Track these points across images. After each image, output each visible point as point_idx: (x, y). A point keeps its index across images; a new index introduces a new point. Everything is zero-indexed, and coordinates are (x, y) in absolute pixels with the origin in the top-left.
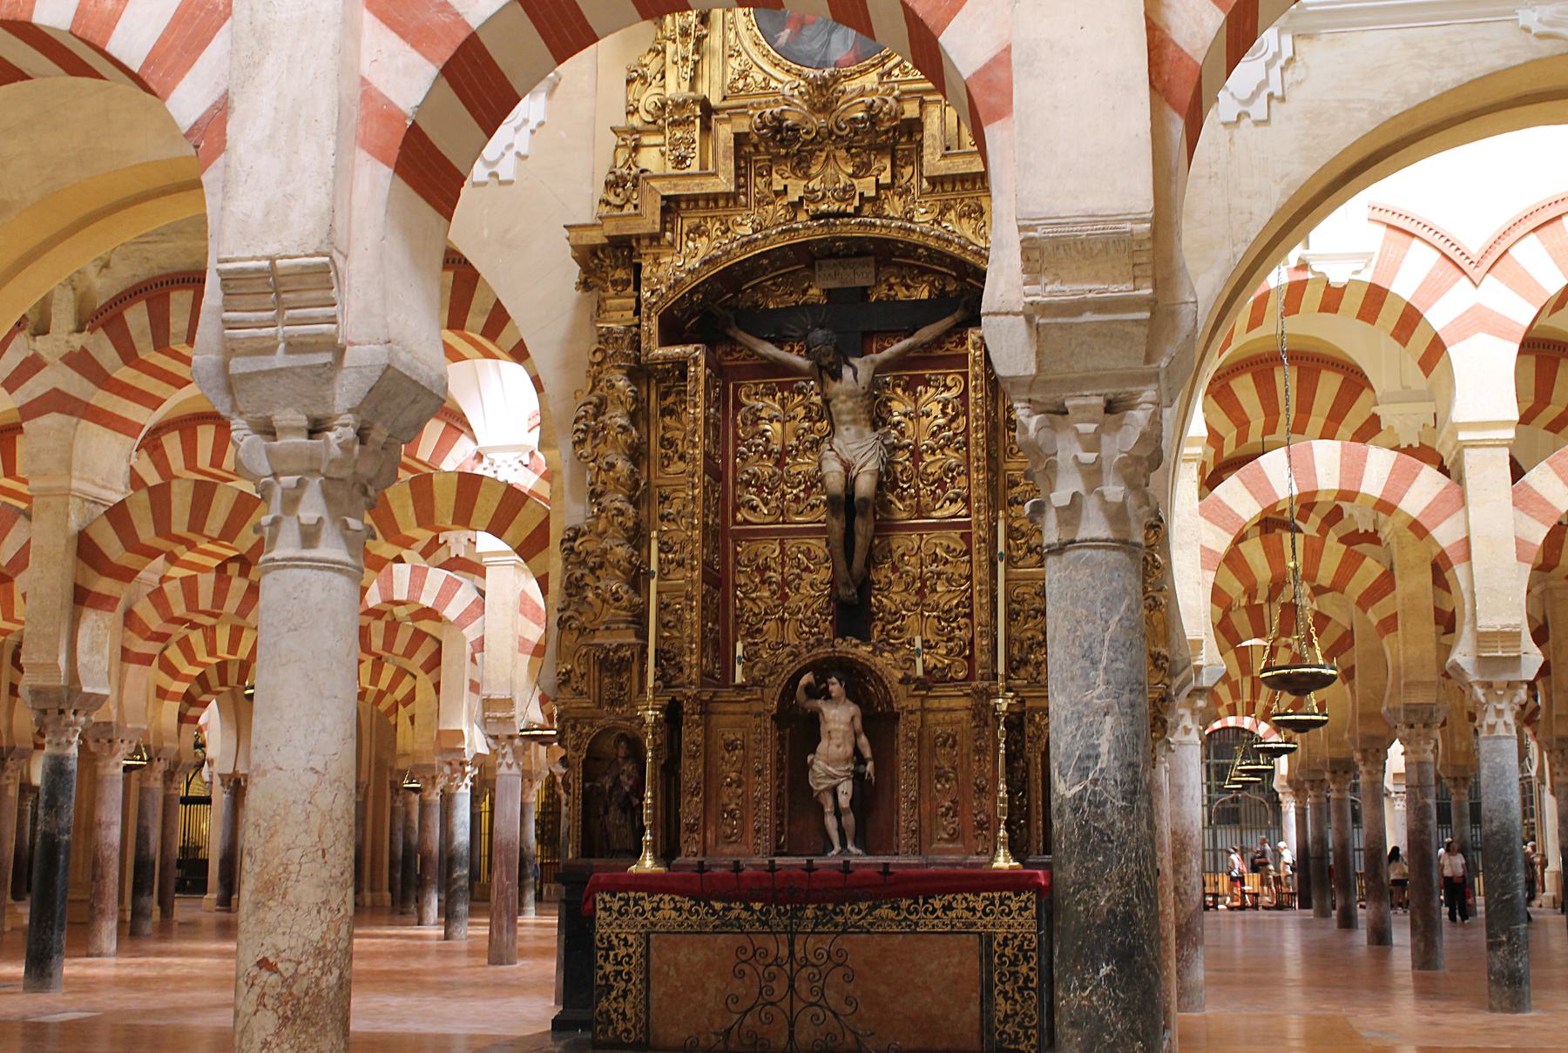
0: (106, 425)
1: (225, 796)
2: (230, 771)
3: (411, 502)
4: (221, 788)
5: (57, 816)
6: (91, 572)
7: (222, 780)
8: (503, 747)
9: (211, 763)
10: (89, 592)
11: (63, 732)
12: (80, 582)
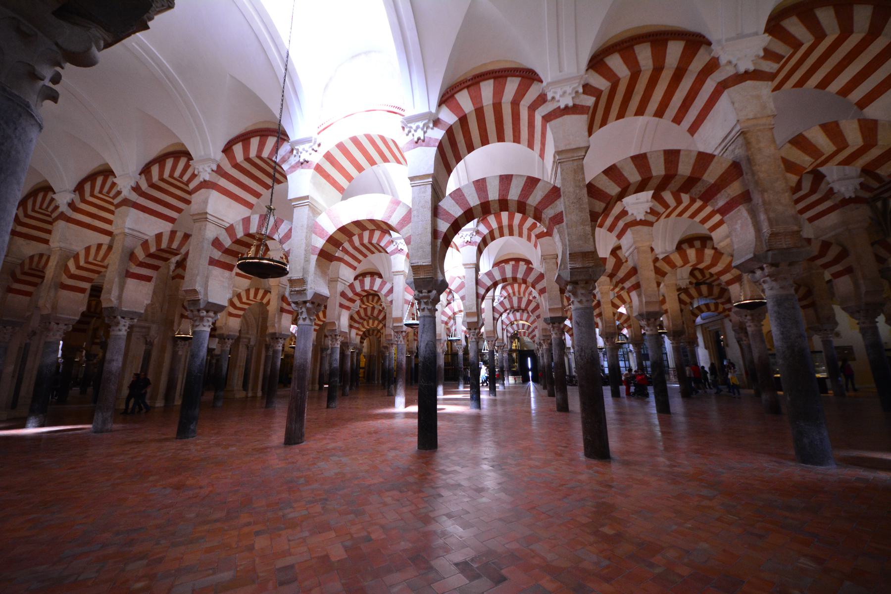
8: (301, 308)
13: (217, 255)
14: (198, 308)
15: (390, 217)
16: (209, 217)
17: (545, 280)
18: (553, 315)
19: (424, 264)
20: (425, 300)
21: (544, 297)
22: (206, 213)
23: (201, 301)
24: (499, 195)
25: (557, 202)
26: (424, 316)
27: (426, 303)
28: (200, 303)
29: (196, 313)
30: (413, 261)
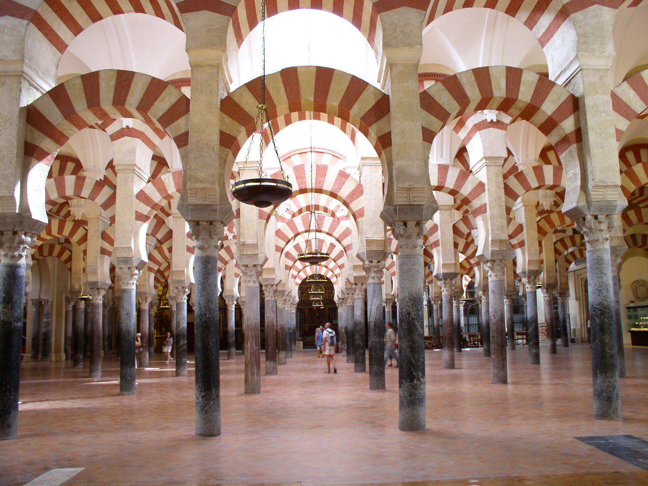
0: (46, 35)
1: (34, 309)
2: (37, 298)
3: (282, 85)
4: (32, 306)
5: (12, 309)
6: (37, 133)
7: (33, 302)
9: (26, 294)
10: (37, 147)
11: (17, 248)
12: (29, 141)
13: (145, 209)
14: (129, 266)
15: (340, 189)
16: (136, 169)
17: (439, 232)
18: (446, 271)
19: (378, 239)
20: (375, 269)
21: (438, 252)
22: (135, 165)
23: (134, 259)
24: (438, 182)
25: (482, 195)
26: (374, 284)
27: (375, 272)
28: (133, 262)
29: (126, 270)
30: (368, 236)
